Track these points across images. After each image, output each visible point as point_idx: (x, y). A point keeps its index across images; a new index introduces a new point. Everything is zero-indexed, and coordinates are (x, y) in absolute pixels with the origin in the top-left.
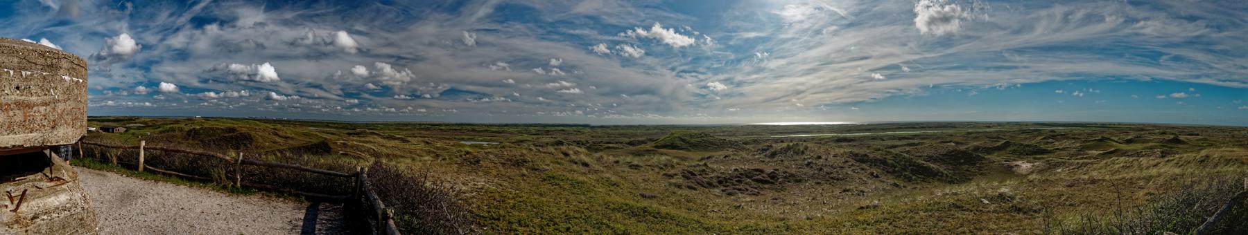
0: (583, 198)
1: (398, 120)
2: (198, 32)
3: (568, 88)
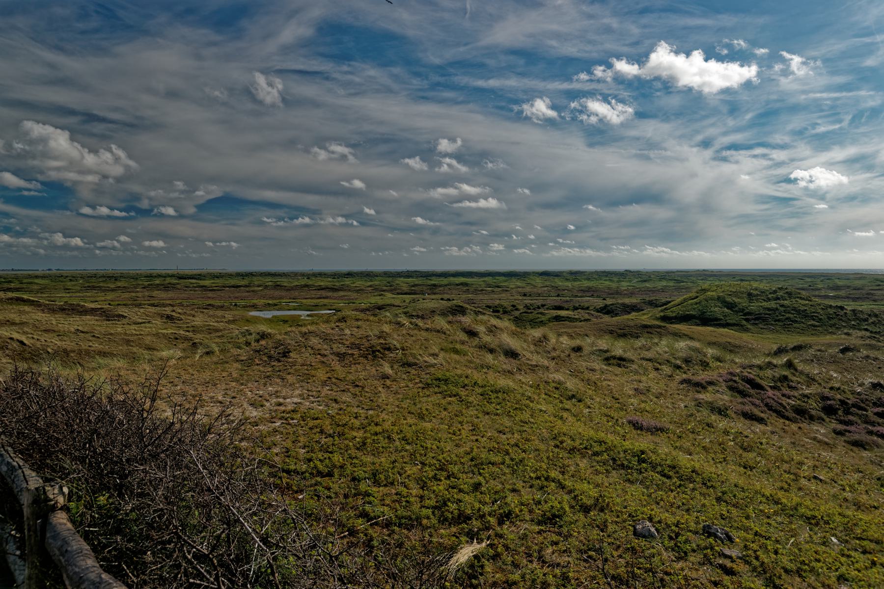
0: (507, 422)
1: (91, 267)
3: (474, 198)
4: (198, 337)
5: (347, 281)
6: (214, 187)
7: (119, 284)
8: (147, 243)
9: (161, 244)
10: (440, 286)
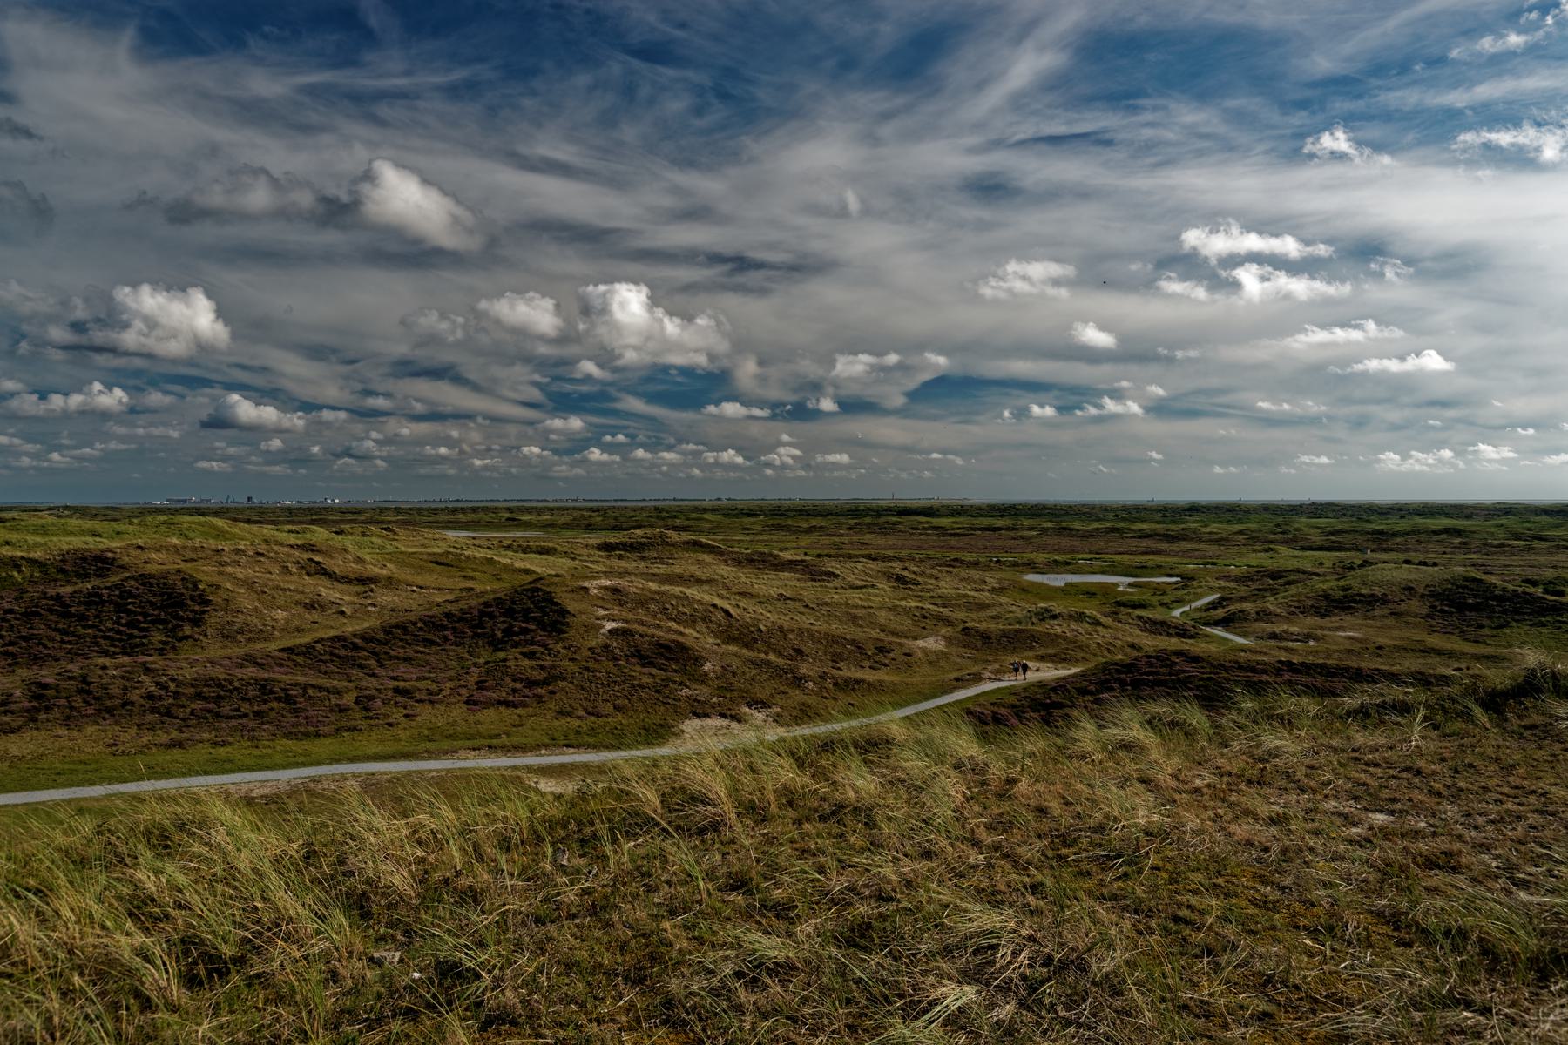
10: (1396, 534)
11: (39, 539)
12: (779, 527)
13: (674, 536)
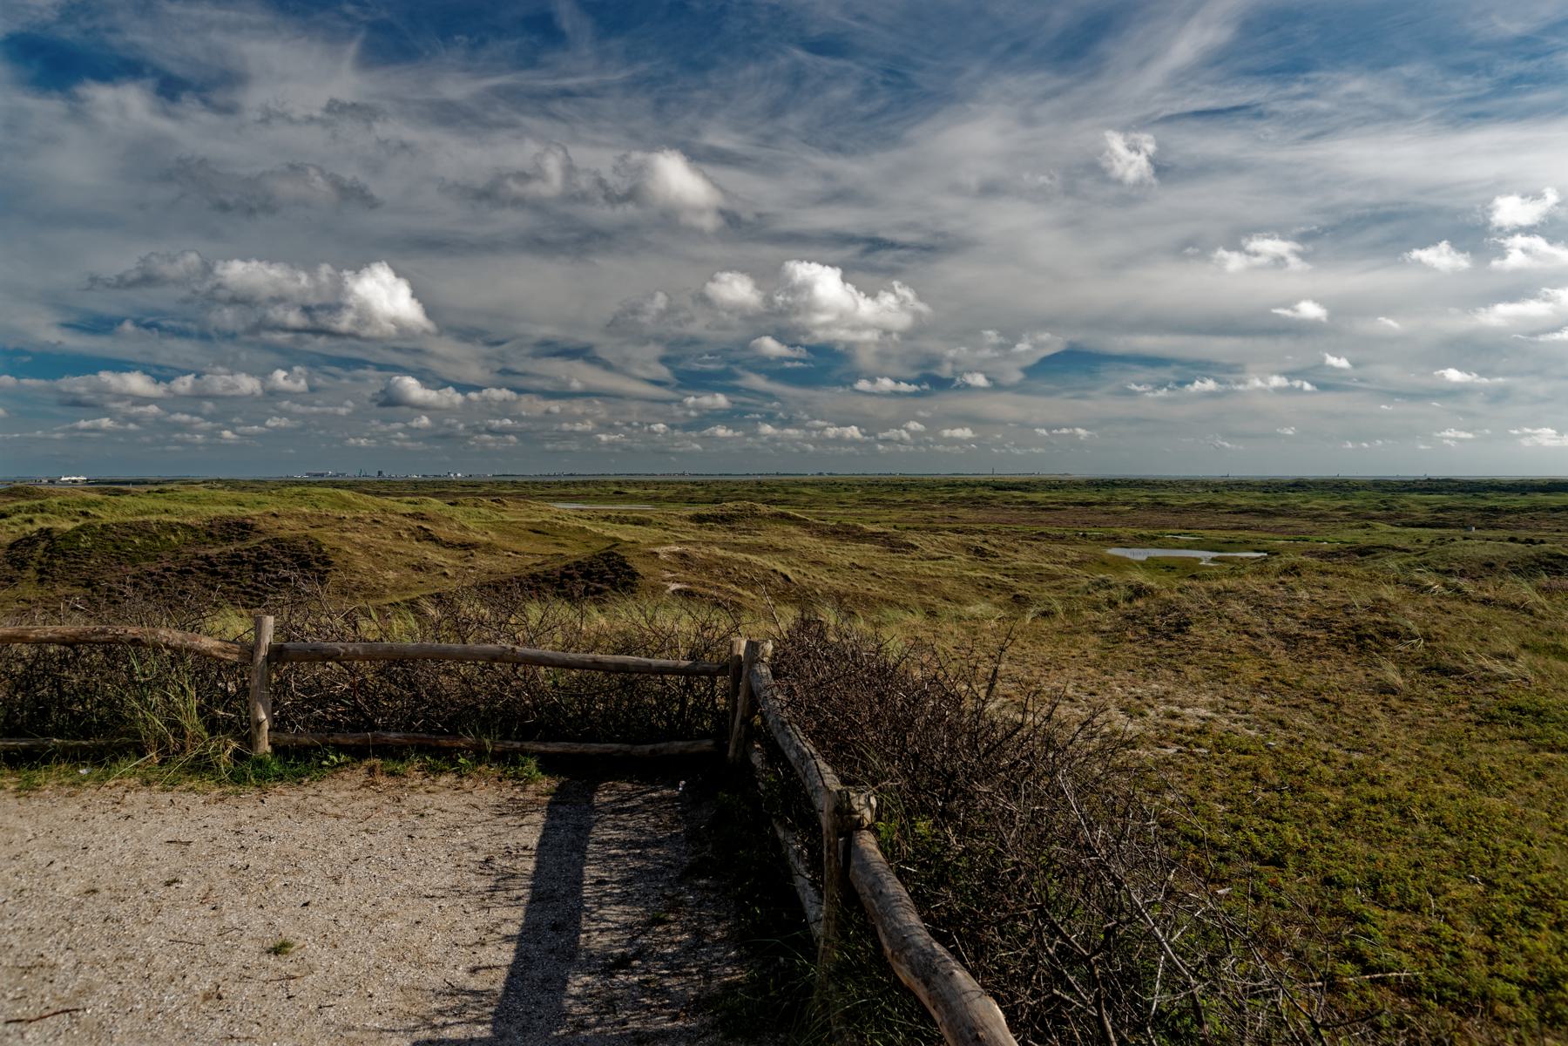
2: (45, 108)
4: (1022, 587)
5: (1294, 499)
6: (1045, 336)
7: (909, 496)
8: (947, 433)
9: (965, 433)
11: (192, 508)
12: (874, 501)
13: (763, 509)
